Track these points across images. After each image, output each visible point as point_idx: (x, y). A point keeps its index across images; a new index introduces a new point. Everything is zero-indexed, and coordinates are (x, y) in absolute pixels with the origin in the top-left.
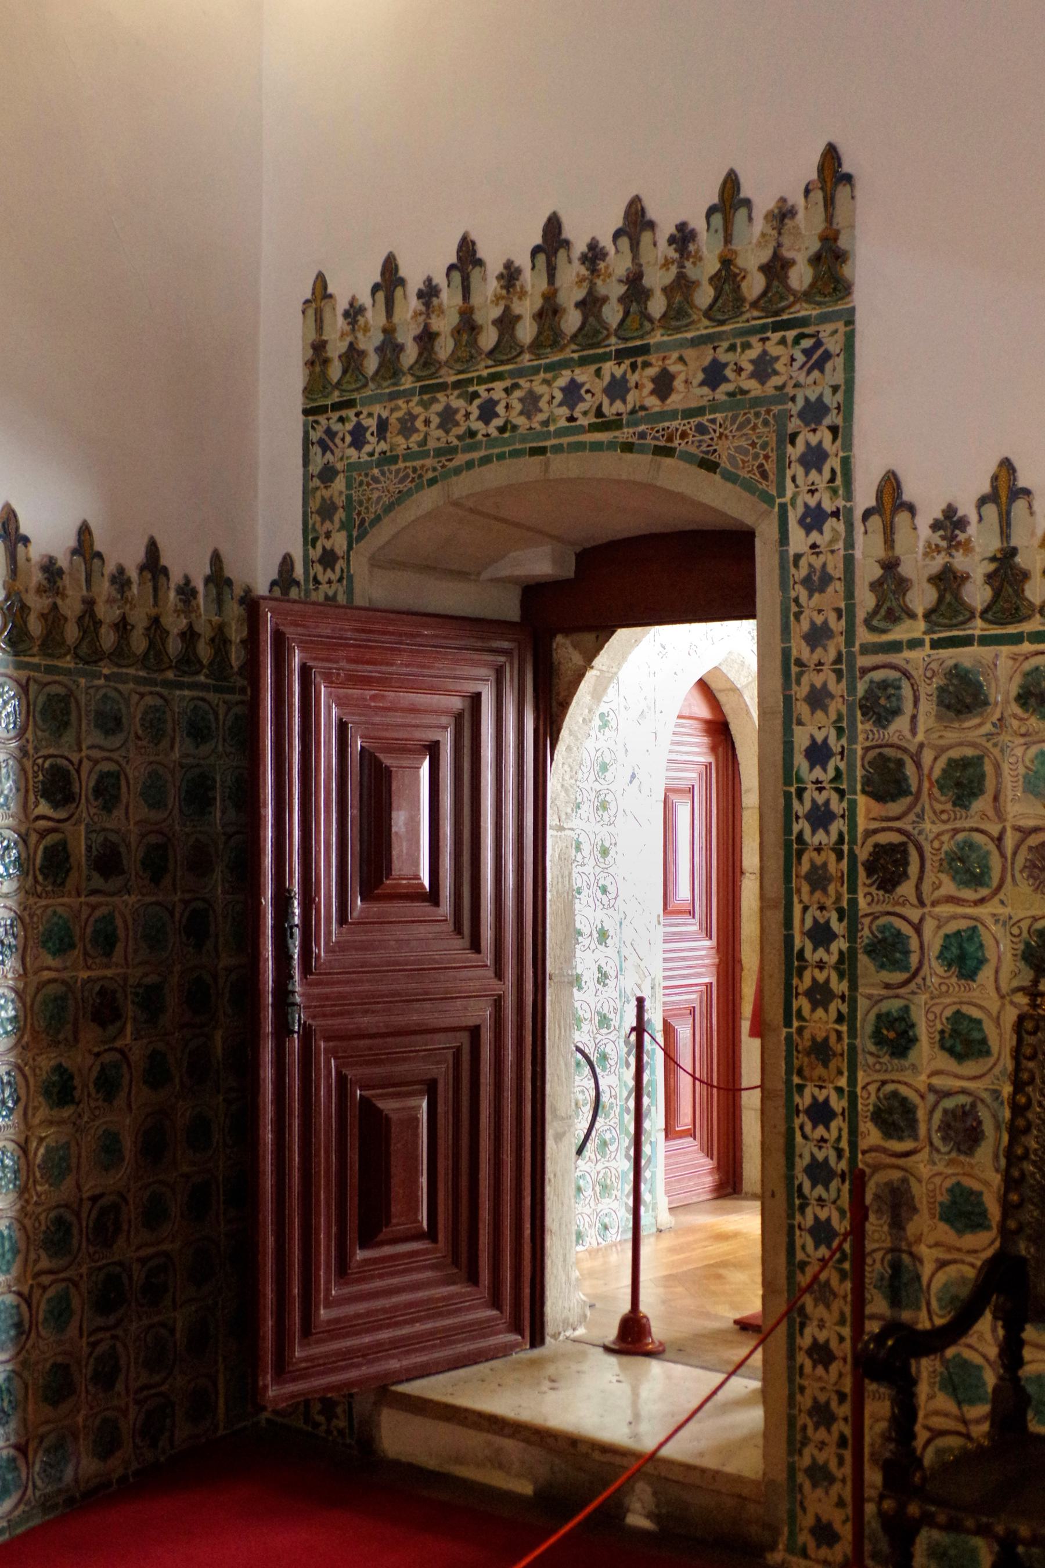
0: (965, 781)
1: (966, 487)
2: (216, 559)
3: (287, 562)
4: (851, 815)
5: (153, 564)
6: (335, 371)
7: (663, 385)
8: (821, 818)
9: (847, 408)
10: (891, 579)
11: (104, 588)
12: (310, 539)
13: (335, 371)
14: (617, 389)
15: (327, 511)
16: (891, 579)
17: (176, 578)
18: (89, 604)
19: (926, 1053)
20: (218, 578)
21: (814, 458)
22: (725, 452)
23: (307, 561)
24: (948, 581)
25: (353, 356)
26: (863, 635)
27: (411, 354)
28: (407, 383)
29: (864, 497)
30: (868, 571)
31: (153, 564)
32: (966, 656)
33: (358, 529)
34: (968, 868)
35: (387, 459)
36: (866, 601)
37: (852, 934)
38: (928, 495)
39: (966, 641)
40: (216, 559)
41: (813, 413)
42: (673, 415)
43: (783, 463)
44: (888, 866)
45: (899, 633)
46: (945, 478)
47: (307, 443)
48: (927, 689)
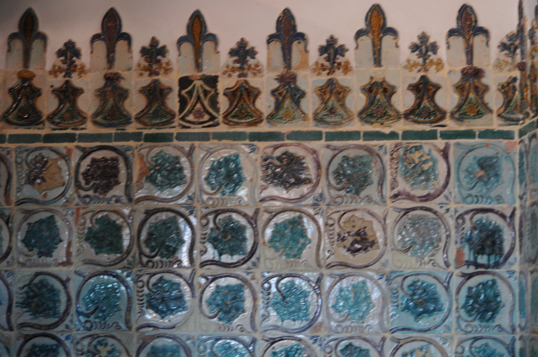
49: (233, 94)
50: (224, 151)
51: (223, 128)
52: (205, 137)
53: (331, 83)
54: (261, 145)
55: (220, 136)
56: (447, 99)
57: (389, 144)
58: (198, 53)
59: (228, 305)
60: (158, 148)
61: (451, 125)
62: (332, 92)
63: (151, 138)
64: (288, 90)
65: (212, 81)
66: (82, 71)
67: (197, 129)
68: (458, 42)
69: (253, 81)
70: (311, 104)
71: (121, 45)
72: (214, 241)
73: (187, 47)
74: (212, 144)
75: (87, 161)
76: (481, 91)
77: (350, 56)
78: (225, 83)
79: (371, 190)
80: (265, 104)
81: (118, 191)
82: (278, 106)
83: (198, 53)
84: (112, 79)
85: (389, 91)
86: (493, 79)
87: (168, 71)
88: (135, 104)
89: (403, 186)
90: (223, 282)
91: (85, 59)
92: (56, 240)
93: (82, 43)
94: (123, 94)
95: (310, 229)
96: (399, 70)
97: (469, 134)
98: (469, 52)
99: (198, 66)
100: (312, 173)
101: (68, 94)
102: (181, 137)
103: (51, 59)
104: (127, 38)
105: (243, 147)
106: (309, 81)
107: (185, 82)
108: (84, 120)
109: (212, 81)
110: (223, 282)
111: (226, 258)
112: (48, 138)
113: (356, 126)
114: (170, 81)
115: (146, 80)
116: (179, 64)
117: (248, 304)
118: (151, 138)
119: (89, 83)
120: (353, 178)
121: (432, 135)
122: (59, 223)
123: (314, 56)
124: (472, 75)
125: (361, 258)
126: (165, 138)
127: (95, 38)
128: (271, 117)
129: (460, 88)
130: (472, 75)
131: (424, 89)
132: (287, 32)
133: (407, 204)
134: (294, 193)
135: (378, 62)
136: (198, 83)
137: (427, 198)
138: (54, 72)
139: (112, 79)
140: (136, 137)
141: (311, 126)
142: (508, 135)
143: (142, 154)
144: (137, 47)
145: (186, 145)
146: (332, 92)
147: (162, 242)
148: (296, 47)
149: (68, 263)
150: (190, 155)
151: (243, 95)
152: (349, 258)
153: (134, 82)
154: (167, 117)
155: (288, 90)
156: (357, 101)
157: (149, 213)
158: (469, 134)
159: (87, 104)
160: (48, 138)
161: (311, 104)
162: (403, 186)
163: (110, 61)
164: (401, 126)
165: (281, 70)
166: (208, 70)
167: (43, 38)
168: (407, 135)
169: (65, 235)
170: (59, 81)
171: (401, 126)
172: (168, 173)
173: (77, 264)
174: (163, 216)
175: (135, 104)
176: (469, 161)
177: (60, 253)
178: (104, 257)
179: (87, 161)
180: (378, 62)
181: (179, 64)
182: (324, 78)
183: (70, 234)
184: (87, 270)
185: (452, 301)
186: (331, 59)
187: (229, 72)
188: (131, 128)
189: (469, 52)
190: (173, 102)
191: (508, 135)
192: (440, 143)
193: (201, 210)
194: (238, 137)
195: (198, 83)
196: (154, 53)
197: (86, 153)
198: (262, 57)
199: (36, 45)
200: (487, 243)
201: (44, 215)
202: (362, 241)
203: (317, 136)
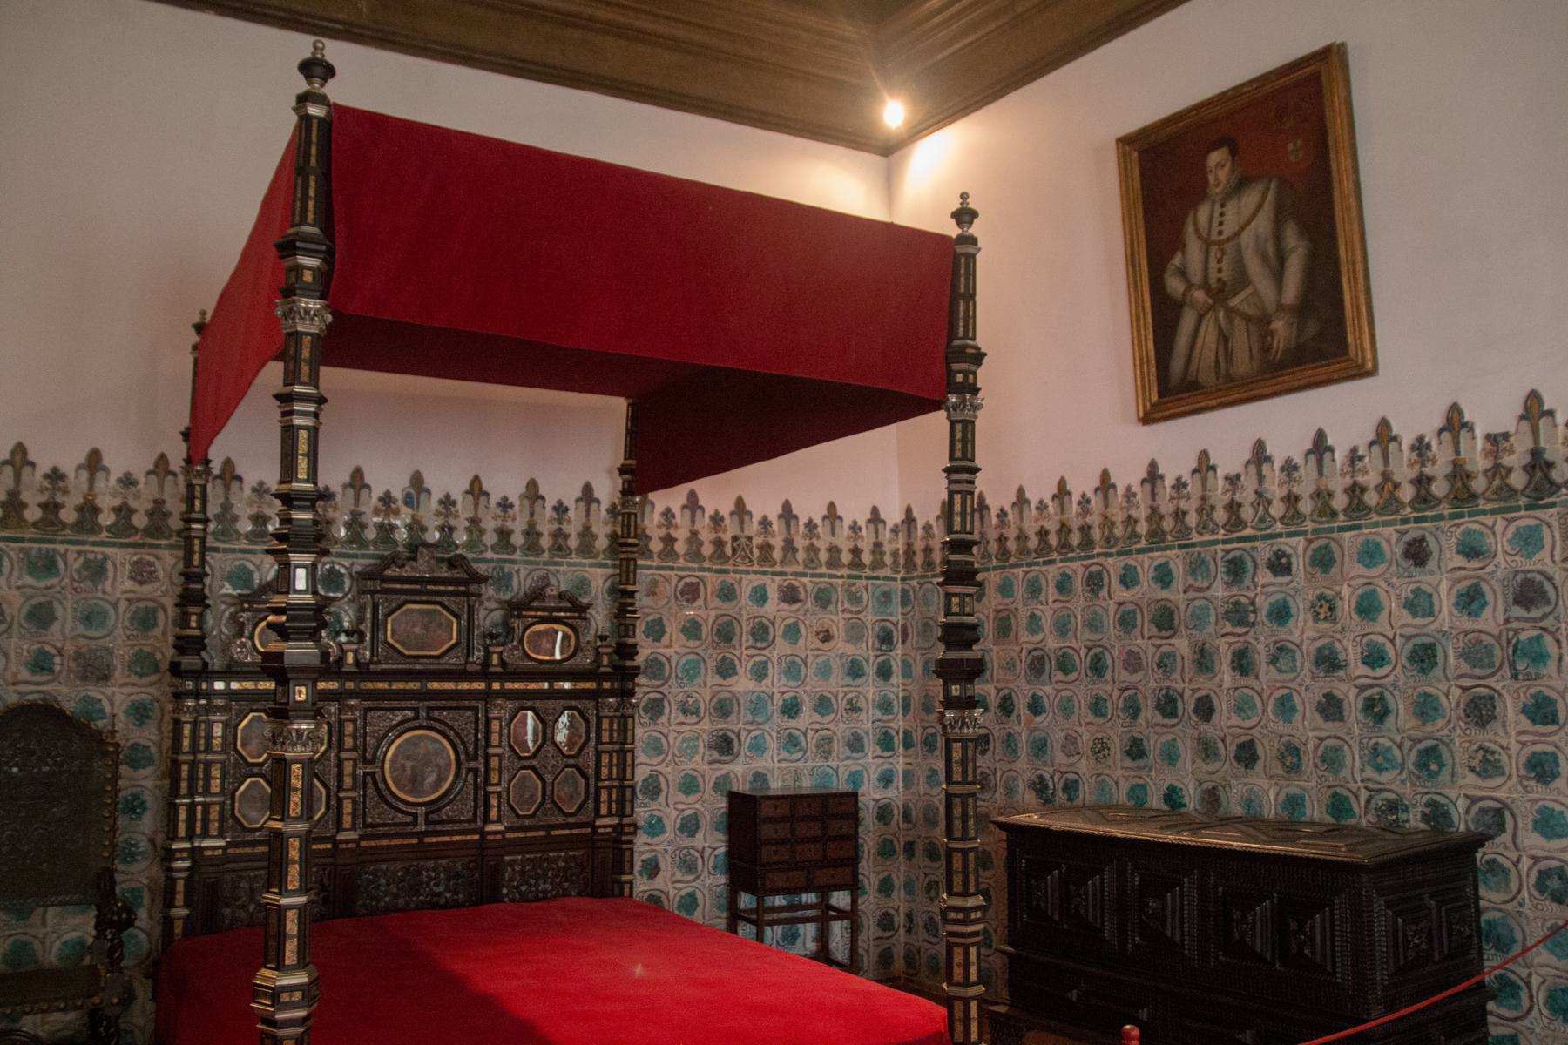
49: (761, 548)
50: (757, 580)
51: (756, 568)
52: (747, 572)
53: (812, 545)
54: (777, 579)
55: (756, 572)
56: (866, 558)
57: (840, 581)
58: (742, 522)
59: (760, 673)
60: (722, 577)
61: (868, 572)
62: (812, 550)
63: (717, 571)
64: (789, 547)
65: (750, 539)
66: (676, 527)
67: (742, 567)
68: (871, 526)
69: (772, 541)
70: (801, 556)
71: (699, 512)
72: (753, 634)
73: (736, 517)
74: (752, 576)
75: (682, 584)
76: (883, 553)
77: (820, 530)
78: (757, 541)
79: (831, 607)
80: (777, 554)
81: (700, 602)
82: (785, 556)
83: (742, 522)
84: (694, 534)
85: (839, 551)
86: (887, 548)
87: (725, 531)
88: (707, 550)
89: (847, 605)
90: (757, 659)
91: (678, 520)
92: (662, 632)
93: (676, 509)
94: (701, 543)
95: (803, 631)
96: (844, 542)
97: (877, 578)
98: (877, 532)
99: (742, 530)
100: (802, 596)
101: (669, 540)
102: (735, 572)
103: (657, 517)
104: (702, 509)
105: (766, 579)
106: (800, 543)
107: (735, 539)
108: (679, 557)
109: (750, 539)
110: (757, 659)
111: (759, 645)
112: (658, 568)
113: (823, 570)
114: (727, 537)
115: (713, 536)
116: (731, 528)
117: (770, 672)
118: (717, 571)
119: (681, 534)
120: (823, 599)
121: (860, 578)
122: (665, 621)
123: (802, 529)
124: (878, 545)
125: (826, 646)
126: (725, 572)
127: (684, 507)
128: (782, 563)
129: (873, 553)
130: (878, 545)
131: (856, 552)
132: (787, 514)
133: (848, 616)
134: (795, 607)
135: (833, 534)
136: (743, 540)
137: (859, 612)
138: (660, 526)
139: (694, 534)
140: (709, 570)
141: (800, 569)
142: (895, 579)
143: (712, 581)
144: (707, 515)
145: (737, 576)
146: (812, 550)
147: (725, 634)
148: (793, 523)
149: (670, 646)
150: (740, 582)
151: (766, 548)
152: (820, 645)
153: (706, 536)
154: (725, 559)
155: (789, 547)
156: (824, 556)
157: (717, 617)
158: (877, 578)
159: (680, 547)
160: (658, 568)
161: (801, 556)
162: (847, 605)
163: (693, 522)
164: (845, 572)
165: (784, 535)
166: (747, 532)
167: (653, 504)
168: (849, 577)
169: (668, 629)
170: (663, 532)
171: (845, 572)
172: (728, 593)
173: (676, 647)
174: (725, 619)
175: (707, 550)
176: (878, 593)
177: (665, 640)
178: (691, 643)
179: (682, 584)
180: (833, 534)
181: (731, 528)
182: (808, 541)
183: (672, 628)
184: (683, 651)
185: (870, 670)
186: (765, 528)
187: (759, 534)
188: (706, 564)
189: (877, 532)
190: (728, 550)
191: (895, 579)
192: (864, 582)
193: (745, 617)
194: (765, 573)
195: (743, 540)
196: (717, 519)
197: (681, 578)
198: (775, 526)
200: (886, 639)
201: (656, 616)
202: (827, 637)
203: (805, 575)
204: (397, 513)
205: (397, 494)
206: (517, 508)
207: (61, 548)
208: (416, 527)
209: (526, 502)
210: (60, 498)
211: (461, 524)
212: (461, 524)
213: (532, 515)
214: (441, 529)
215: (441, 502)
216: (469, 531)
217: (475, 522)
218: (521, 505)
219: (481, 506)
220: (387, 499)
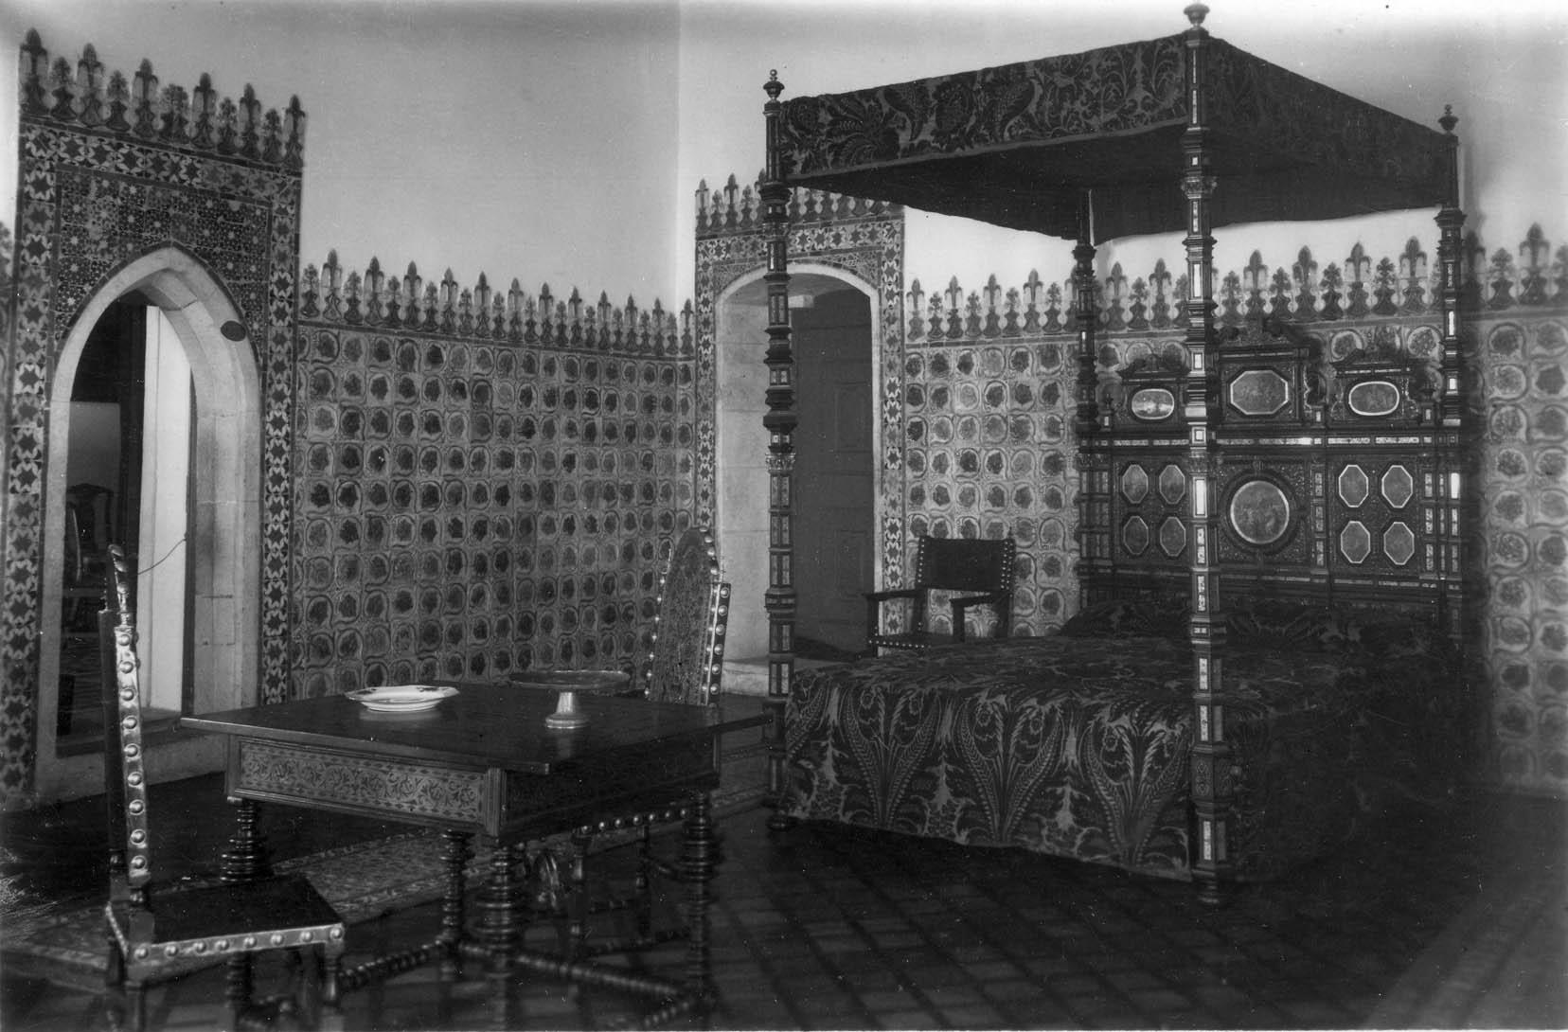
0: (941, 397)
1: (941, 287)
2: (658, 303)
3: (688, 304)
4: (903, 411)
5: (631, 307)
6: (709, 222)
7: (837, 239)
8: (893, 412)
9: (902, 253)
10: (916, 323)
11: (611, 318)
12: (698, 294)
13: (709, 222)
14: (820, 239)
15: (705, 282)
16: (916, 323)
17: (640, 311)
18: (606, 325)
19: (930, 504)
20: (658, 311)
21: (890, 272)
22: (859, 267)
23: (697, 304)
24: (935, 321)
25: (716, 216)
26: (907, 341)
27: (740, 218)
28: (738, 229)
29: (908, 288)
30: (908, 317)
31: (631, 307)
32: (940, 350)
33: (718, 289)
34: (942, 430)
35: (729, 261)
36: (908, 328)
37: (904, 458)
38: (929, 290)
39: (941, 345)
40: (658, 303)
41: (891, 254)
42: (840, 251)
43: (880, 273)
44: (916, 431)
45: (919, 341)
46: (934, 285)
47: (697, 252)
48: (928, 362)
199: (1542, 250)
204: (1288, 287)
205: (1289, 271)
206: (1397, 269)
207: (1059, 344)
208: (1306, 299)
209: (1406, 262)
210: (1057, 306)
211: (1345, 290)
212: (1345, 290)
213: (1413, 273)
214: (1326, 297)
215: (1326, 273)
216: (1351, 296)
217: (1357, 286)
218: (1402, 265)
219: (1363, 272)
220: (1280, 276)
